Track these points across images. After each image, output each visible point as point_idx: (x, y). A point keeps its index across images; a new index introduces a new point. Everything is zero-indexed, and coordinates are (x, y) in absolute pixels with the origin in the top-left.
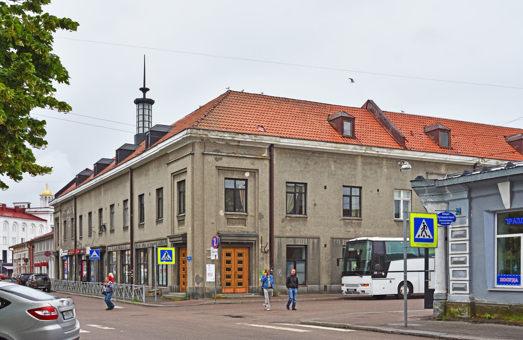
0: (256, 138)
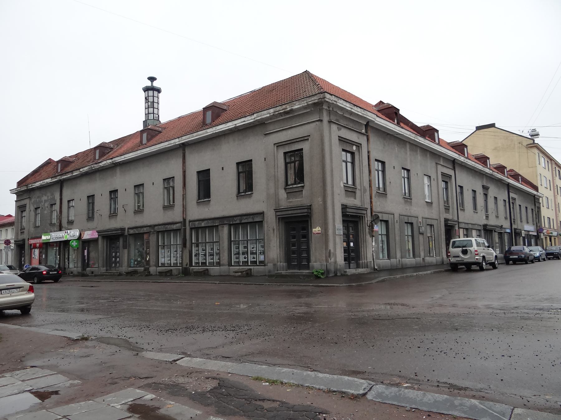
0: (365, 113)
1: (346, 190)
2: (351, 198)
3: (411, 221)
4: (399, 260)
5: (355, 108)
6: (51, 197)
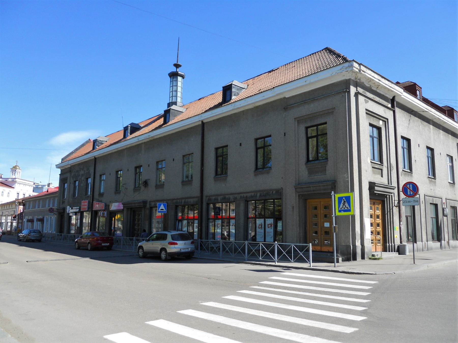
1: (373, 167)
2: (378, 175)
3: (436, 202)
4: (425, 243)
5: (383, 80)
6: (87, 172)
